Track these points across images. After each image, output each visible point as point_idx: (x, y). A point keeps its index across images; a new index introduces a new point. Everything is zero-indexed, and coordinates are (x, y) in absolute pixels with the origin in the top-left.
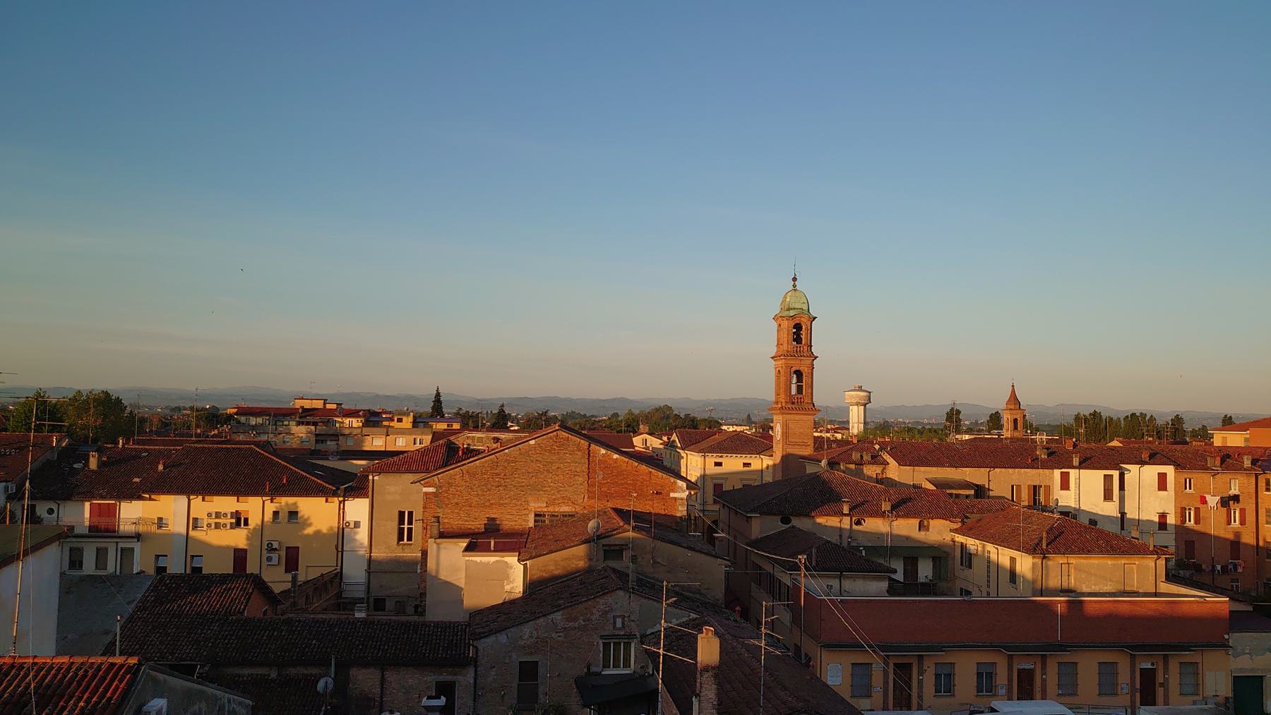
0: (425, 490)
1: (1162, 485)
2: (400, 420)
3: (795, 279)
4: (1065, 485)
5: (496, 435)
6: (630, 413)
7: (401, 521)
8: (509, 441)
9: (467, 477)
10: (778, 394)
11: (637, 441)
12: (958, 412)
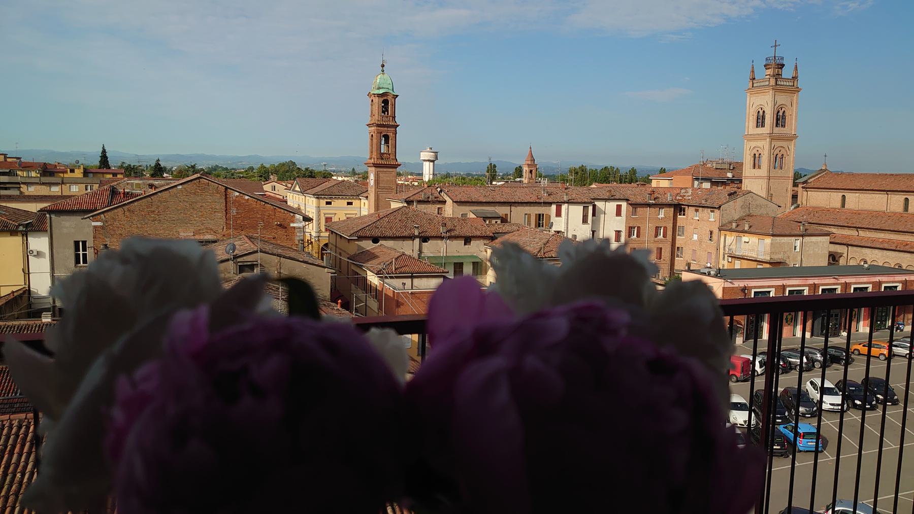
0: (94, 224)
1: (619, 213)
2: (72, 171)
3: (383, 66)
4: (558, 214)
6: (263, 167)
7: (77, 249)
8: (162, 186)
9: (127, 213)
10: (372, 152)
11: (267, 187)
12: (495, 166)
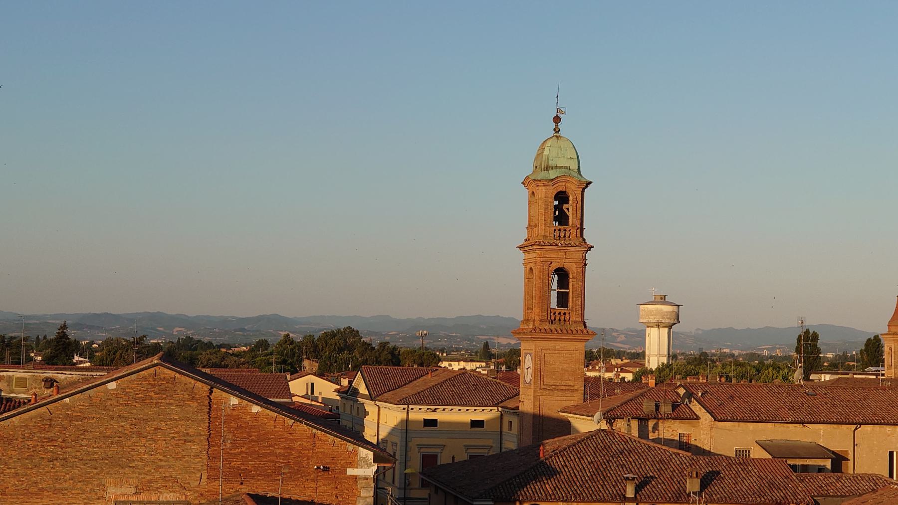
3: (557, 119)
5: (50, 374)
8: (72, 384)
10: (528, 308)
11: (298, 387)
12: (815, 337)
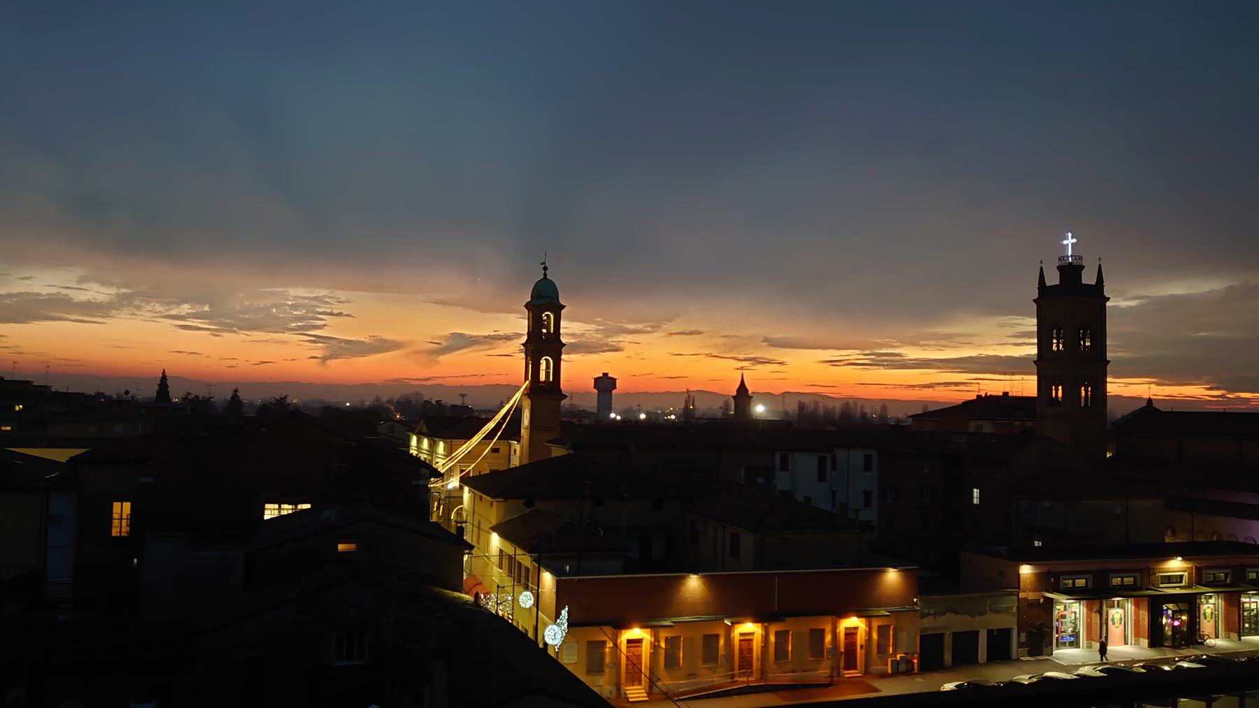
1: (868, 467)
4: (784, 467)
6: (378, 399)
